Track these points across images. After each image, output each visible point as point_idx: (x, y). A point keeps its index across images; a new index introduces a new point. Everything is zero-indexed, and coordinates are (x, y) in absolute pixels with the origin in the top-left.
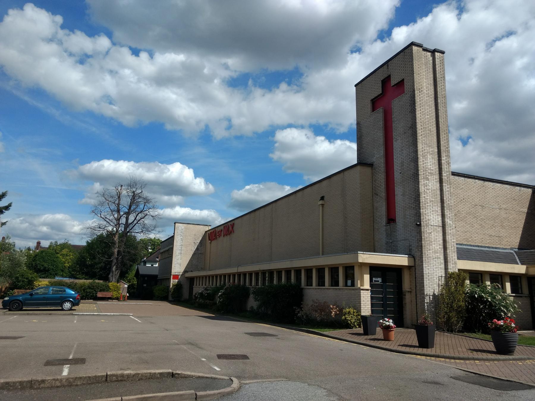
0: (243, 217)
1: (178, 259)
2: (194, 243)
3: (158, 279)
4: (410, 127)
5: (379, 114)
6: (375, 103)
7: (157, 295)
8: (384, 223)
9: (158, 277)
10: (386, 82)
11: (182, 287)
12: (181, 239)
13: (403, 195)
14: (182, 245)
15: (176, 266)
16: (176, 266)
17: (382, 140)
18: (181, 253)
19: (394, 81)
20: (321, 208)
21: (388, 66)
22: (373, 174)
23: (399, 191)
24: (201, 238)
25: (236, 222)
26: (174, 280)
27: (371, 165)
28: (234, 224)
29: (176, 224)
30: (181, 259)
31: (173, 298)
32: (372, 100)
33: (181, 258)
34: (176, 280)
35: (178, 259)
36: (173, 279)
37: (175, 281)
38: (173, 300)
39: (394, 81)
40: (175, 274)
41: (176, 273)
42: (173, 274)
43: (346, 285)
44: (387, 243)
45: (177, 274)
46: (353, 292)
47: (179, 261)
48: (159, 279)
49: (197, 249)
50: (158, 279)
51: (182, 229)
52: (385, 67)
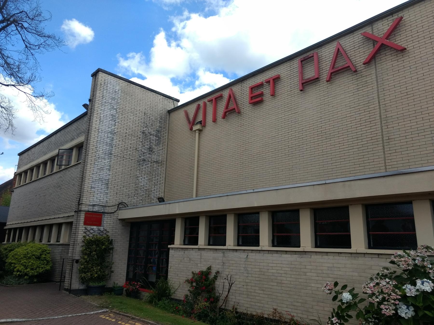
1: (101, 169)
2: (143, 133)
3: (5, 228)
7: (18, 271)
9: (7, 224)
11: (112, 249)
12: (112, 115)
14: (113, 133)
15: (94, 188)
16: (94, 188)
18: (111, 154)
26: (89, 227)
29: (101, 75)
30: (109, 170)
31: (83, 280)
33: (110, 166)
34: (95, 227)
35: (101, 169)
36: (85, 223)
37: (92, 229)
38: (82, 287)
40: (91, 209)
41: (94, 205)
42: (86, 209)
45: (96, 209)
47: (105, 174)
48: (10, 230)
50: (5, 228)
51: (115, 92)
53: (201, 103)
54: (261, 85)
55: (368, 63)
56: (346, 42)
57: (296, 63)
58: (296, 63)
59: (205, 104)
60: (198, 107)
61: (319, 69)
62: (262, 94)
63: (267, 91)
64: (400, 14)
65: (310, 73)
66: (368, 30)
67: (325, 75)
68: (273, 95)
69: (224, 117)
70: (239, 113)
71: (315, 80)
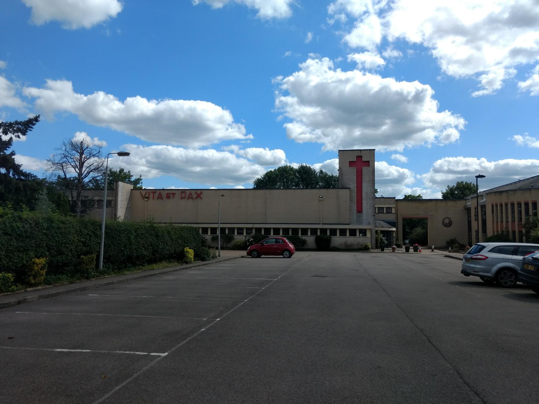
4: (372, 181)
5: (354, 170)
6: (351, 164)
8: (356, 212)
13: (367, 204)
17: (356, 180)
19: (363, 160)
21: (361, 152)
22: (350, 192)
23: (364, 203)
25: (203, 191)
27: (349, 188)
28: (201, 193)
32: (350, 162)
39: (363, 160)
43: (359, 236)
46: (365, 238)
52: (360, 151)
54: (170, 194)
55: (195, 198)
56: (192, 192)
57: (180, 191)
58: (180, 191)
59: (149, 192)
60: (146, 193)
61: (185, 195)
63: (172, 196)
64: (202, 191)
65: (183, 196)
66: (196, 191)
67: (187, 198)
68: (173, 198)
69: (157, 199)
70: (162, 199)
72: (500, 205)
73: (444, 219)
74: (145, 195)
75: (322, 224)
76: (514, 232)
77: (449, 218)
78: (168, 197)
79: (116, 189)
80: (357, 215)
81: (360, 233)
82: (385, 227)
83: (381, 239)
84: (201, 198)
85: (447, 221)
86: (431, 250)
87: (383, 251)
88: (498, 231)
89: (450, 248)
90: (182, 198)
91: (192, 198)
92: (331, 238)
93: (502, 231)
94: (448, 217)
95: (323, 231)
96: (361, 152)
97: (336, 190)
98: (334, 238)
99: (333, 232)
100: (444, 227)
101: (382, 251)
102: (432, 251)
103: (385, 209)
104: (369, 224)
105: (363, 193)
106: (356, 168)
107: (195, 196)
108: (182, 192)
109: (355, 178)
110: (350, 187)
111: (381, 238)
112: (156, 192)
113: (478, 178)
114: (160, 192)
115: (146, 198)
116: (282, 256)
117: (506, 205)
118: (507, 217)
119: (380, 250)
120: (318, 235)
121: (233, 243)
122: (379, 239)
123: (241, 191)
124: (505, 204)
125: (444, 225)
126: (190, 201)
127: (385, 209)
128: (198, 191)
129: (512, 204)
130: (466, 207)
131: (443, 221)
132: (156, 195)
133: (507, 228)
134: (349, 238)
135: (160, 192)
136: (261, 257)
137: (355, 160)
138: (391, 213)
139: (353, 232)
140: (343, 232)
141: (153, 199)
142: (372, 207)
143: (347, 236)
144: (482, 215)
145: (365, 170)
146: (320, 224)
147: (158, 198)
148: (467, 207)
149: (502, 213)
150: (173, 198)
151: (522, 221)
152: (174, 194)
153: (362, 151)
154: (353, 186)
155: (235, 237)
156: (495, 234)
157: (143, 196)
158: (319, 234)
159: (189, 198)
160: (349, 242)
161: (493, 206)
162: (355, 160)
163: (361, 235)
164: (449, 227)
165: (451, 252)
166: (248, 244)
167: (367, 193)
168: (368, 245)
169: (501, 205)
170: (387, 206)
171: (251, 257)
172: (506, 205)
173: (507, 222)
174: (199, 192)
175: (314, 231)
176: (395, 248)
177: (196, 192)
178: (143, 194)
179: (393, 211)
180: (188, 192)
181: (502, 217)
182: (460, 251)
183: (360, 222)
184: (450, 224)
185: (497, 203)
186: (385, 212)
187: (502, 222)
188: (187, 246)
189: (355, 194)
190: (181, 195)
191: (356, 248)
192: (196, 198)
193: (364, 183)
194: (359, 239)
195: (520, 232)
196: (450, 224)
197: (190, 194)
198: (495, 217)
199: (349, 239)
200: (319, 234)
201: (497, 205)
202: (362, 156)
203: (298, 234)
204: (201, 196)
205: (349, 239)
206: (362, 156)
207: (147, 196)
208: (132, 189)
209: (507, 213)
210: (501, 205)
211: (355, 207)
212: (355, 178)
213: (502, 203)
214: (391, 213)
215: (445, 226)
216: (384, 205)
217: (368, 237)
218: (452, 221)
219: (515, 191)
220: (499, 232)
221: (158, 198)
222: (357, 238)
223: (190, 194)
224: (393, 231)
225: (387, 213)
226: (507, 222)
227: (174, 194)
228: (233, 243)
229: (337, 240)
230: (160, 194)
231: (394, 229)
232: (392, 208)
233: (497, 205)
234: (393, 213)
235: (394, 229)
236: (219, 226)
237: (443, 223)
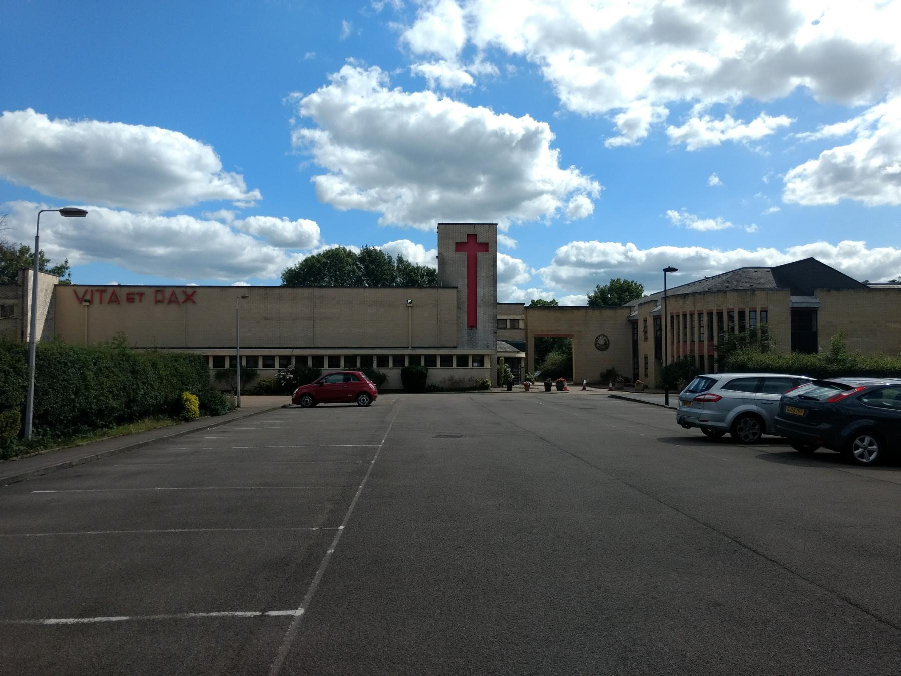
0: (226, 289)
4: (492, 276)
5: (463, 257)
6: (459, 246)
10: (472, 237)
13: (484, 314)
17: (466, 275)
20: (410, 309)
21: (474, 227)
24: (51, 295)
25: (197, 290)
27: (456, 288)
28: (195, 292)
32: (456, 243)
44: (468, 340)
46: (483, 370)
49: (48, 312)
53: (89, 289)
54: (133, 294)
55: (183, 303)
56: (176, 290)
57: (153, 290)
58: (153, 290)
59: (92, 291)
62: (134, 299)
63: (137, 298)
65: (160, 297)
66: (184, 289)
67: (166, 301)
69: (109, 303)
70: (119, 304)
71: (162, 302)
72: (682, 315)
73: (597, 338)
74: (84, 296)
75: (412, 347)
76: (702, 357)
77: (606, 337)
78: (130, 299)
79: (23, 283)
80: (467, 332)
81: (473, 361)
82: (510, 352)
83: (506, 371)
84: (194, 302)
85: (601, 341)
86: (581, 387)
87: (511, 390)
88: (679, 356)
89: (610, 383)
90: (157, 302)
91: (177, 302)
92: (427, 370)
93: (686, 356)
94: (604, 335)
95: (415, 359)
96: (474, 227)
97: (436, 290)
98: (432, 370)
99: (431, 360)
100: (599, 351)
101: (508, 390)
102: (583, 389)
103: (508, 322)
104: (487, 347)
105: (477, 295)
106: (466, 255)
107: (181, 298)
108: (157, 292)
109: (465, 270)
110: (458, 285)
111: (505, 369)
112: (105, 291)
113: (667, 273)
114: (114, 290)
115: (85, 301)
116: (356, 404)
117: (692, 315)
118: (692, 335)
119: (506, 389)
120: (406, 366)
121: (254, 383)
122: (503, 371)
123: (268, 291)
124: (690, 314)
125: (597, 348)
126: (174, 306)
127: (508, 322)
128: (188, 289)
129: (700, 314)
130: (630, 318)
131: (596, 341)
132: (107, 296)
133: (692, 350)
134: (456, 370)
135: (114, 290)
136: (317, 405)
137: (465, 240)
138: (518, 329)
139: (462, 361)
140: (446, 361)
141: (101, 303)
142: (491, 319)
143: (469, 367)
144: (656, 332)
145: (481, 257)
146: (408, 347)
147: (110, 302)
148: (632, 319)
149: (685, 328)
150: (140, 301)
151: (713, 340)
152: (141, 295)
153: (476, 226)
154: (462, 284)
155: (259, 372)
156: (675, 360)
157: (78, 298)
158: (407, 364)
159: (170, 302)
160: (456, 377)
161: (672, 317)
162: (465, 240)
163: (475, 364)
164: (604, 350)
165: (613, 390)
166: (283, 384)
167: (484, 295)
168: (486, 381)
169: (685, 316)
170: (511, 317)
171: (300, 405)
172: (692, 315)
173: (693, 341)
174: (190, 291)
175: (399, 359)
176: (530, 385)
177: (183, 292)
178: (81, 294)
179: (521, 326)
180: (168, 292)
181: (685, 335)
182: (624, 387)
183: (472, 343)
184: (605, 347)
185: (679, 313)
186: (508, 327)
187: (685, 341)
188: (187, 390)
189: (465, 299)
190: (156, 297)
191: (468, 386)
192: (184, 302)
193: (479, 279)
194: (471, 372)
195: (711, 356)
196: (605, 347)
197: (173, 294)
198: (675, 335)
199: (456, 372)
200: (407, 364)
201: (679, 316)
202: (476, 235)
203: (372, 365)
204: (195, 298)
205: (456, 372)
206: (476, 235)
207: (88, 297)
208: (55, 286)
209: (692, 328)
210: (685, 316)
211: (465, 319)
212: (465, 270)
213: (686, 312)
214: (518, 329)
215: (599, 349)
216: (507, 315)
217: (488, 367)
218: (608, 341)
219: (704, 295)
220: (681, 358)
221: (110, 302)
222: (469, 370)
223: (173, 294)
224: (519, 358)
225: (512, 328)
226: (693, 341)
227: (141, 295)
228: (254, 383)
229: (437, 374)
230: (114, 293)
231: (523, 355)
232: (519, 320)
233: (678, 316)
234: (521, 329)
235: (523, 355)
236: (237, 353)
237: (595, 344)
